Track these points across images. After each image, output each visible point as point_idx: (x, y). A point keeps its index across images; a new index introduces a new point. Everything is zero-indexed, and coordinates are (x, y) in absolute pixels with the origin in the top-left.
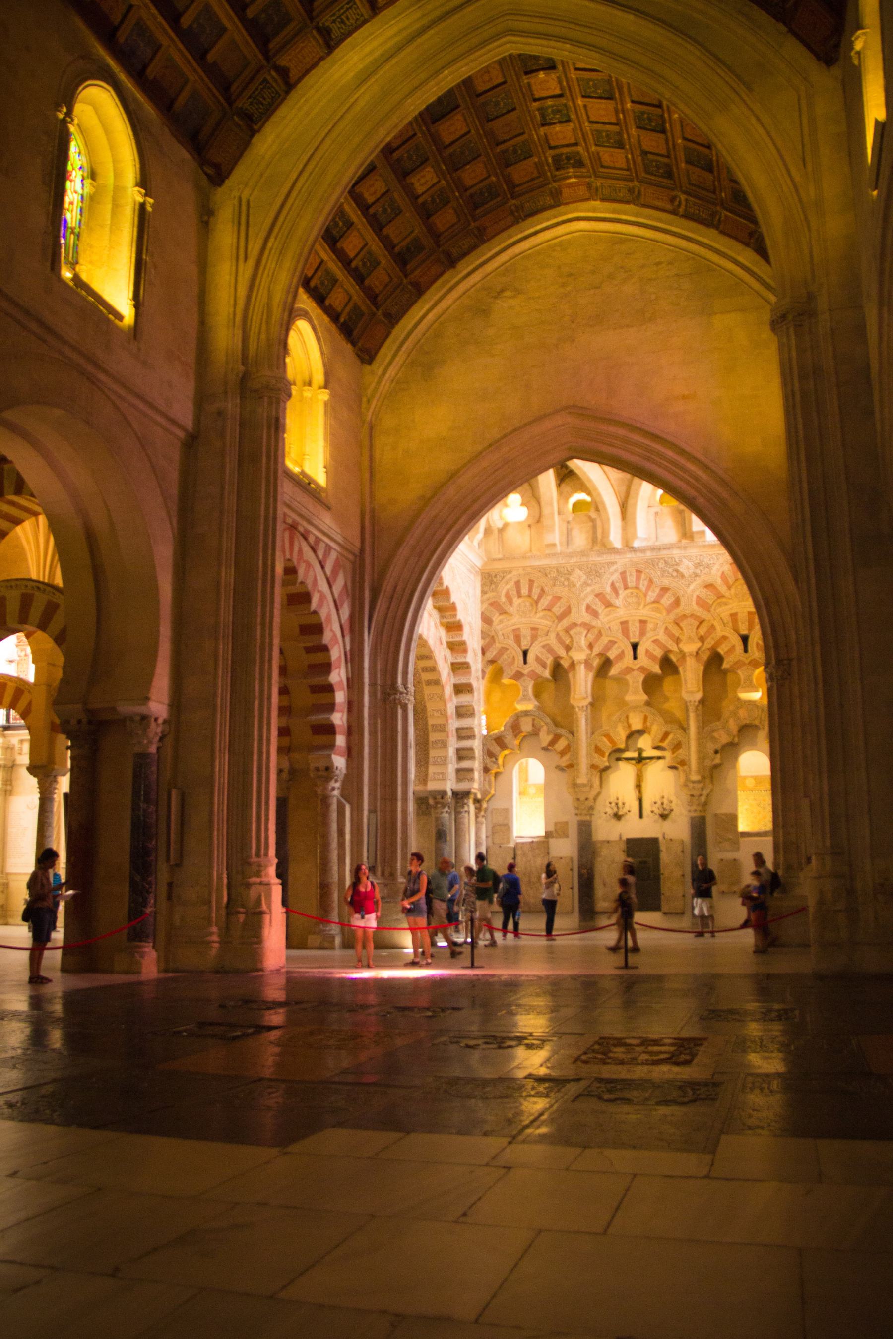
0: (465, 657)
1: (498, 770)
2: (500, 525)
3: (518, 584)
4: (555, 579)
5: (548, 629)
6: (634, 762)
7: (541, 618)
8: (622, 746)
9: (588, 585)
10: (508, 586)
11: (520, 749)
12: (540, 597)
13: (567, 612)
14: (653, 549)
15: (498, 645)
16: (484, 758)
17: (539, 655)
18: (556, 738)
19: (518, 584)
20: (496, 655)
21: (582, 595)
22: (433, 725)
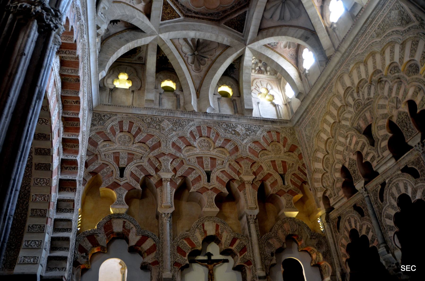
3: (121, 123)
4: (149, 124)
5: (141, 155)
6: (206, 264)
7: (137, 147)
8: (200, 248)
9: (174, 131)
12: (137, 133)
13: (159, 145)
14: (219, 116)
15: (100, 161)
17: (134, 172)
18: (144, 238)
19: (121, 123)
20: (97, 168)
21: (169, 136)
22: (33, 210)
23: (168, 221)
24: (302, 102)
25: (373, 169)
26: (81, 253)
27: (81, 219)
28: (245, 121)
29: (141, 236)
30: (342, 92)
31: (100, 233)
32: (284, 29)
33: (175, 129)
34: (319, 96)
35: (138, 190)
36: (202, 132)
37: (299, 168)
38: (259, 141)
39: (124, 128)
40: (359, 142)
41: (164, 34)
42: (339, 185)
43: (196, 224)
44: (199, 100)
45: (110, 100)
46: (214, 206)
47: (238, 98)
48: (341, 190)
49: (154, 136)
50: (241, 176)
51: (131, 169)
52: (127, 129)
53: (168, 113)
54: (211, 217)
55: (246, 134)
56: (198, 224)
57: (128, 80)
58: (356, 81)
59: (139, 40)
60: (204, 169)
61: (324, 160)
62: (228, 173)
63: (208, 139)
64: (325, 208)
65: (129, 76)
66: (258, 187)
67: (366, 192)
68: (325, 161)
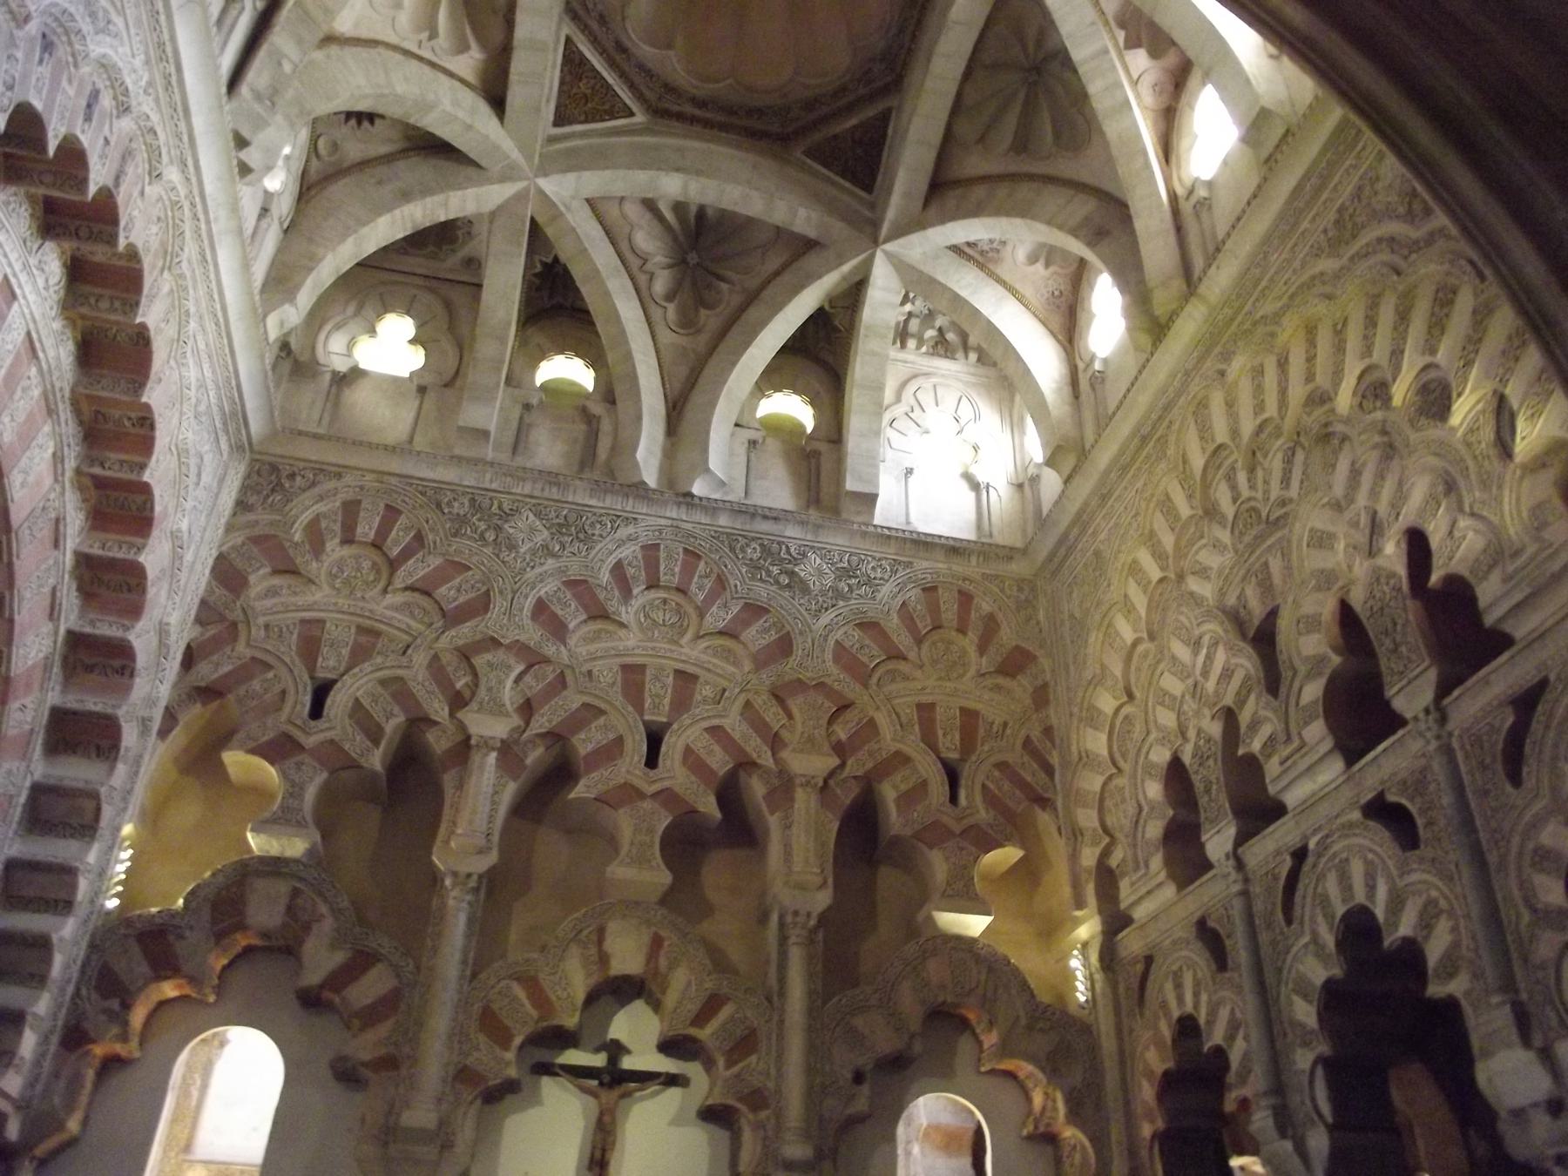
0: (127, 629)
1: (119, 1048)
2: (341, 366)
3: (351, 510)
4: (462, 520)
6: (595, 1083)
7: (396, 609)
8: (571, 1021)
9: (554, 555)
10: (321, 508)
11: (219, 990)
12: (407, 554)
13: (481, 605)
16: (77, 993)
17: (366, 702)
18: (361, 962)
19: (351, 510)
20: (226, 675)
21: (530, 575)
23: (465, 905)
24: (1067, 481)
25: (1265, 790)
26: (105, 997)
27: (129, 864)
28: (840, 541)
29: (349, 954)
30: (1198, 461)
31: (191, 928)
32: (1024, 191)
33: (557, 548)
34: (1125, 469)
35: (374, 774)
36: (662, 568)
37: (1027, 742)
38: (881, 622)
39: (359, 530)
40: (1233, 672)
41: (556, 178)
42: (1154, 829)
43: (571, 925)
44: (673, 445)
45: (326, 415)
46: (654, 863)
47: (832, 445)
48: (1157, 850)
49: (469, 568)
50: (785, 754)
51: (358, 689)
52: (373, 533)
53: (539, 486)
54: (637, 903)
55: (834, 589)
56: (578, 927)
57: (413, 342)
58: (1247, 427)
59: (451, 194)
60: (641, 714)
61: (1118, 723)
62: (737, 736)
63: (679, 598)
64: (1100, 912)
65: (419, 327)
66: (848, 802)
67: (1240, 877)
68: (1118, 732)
